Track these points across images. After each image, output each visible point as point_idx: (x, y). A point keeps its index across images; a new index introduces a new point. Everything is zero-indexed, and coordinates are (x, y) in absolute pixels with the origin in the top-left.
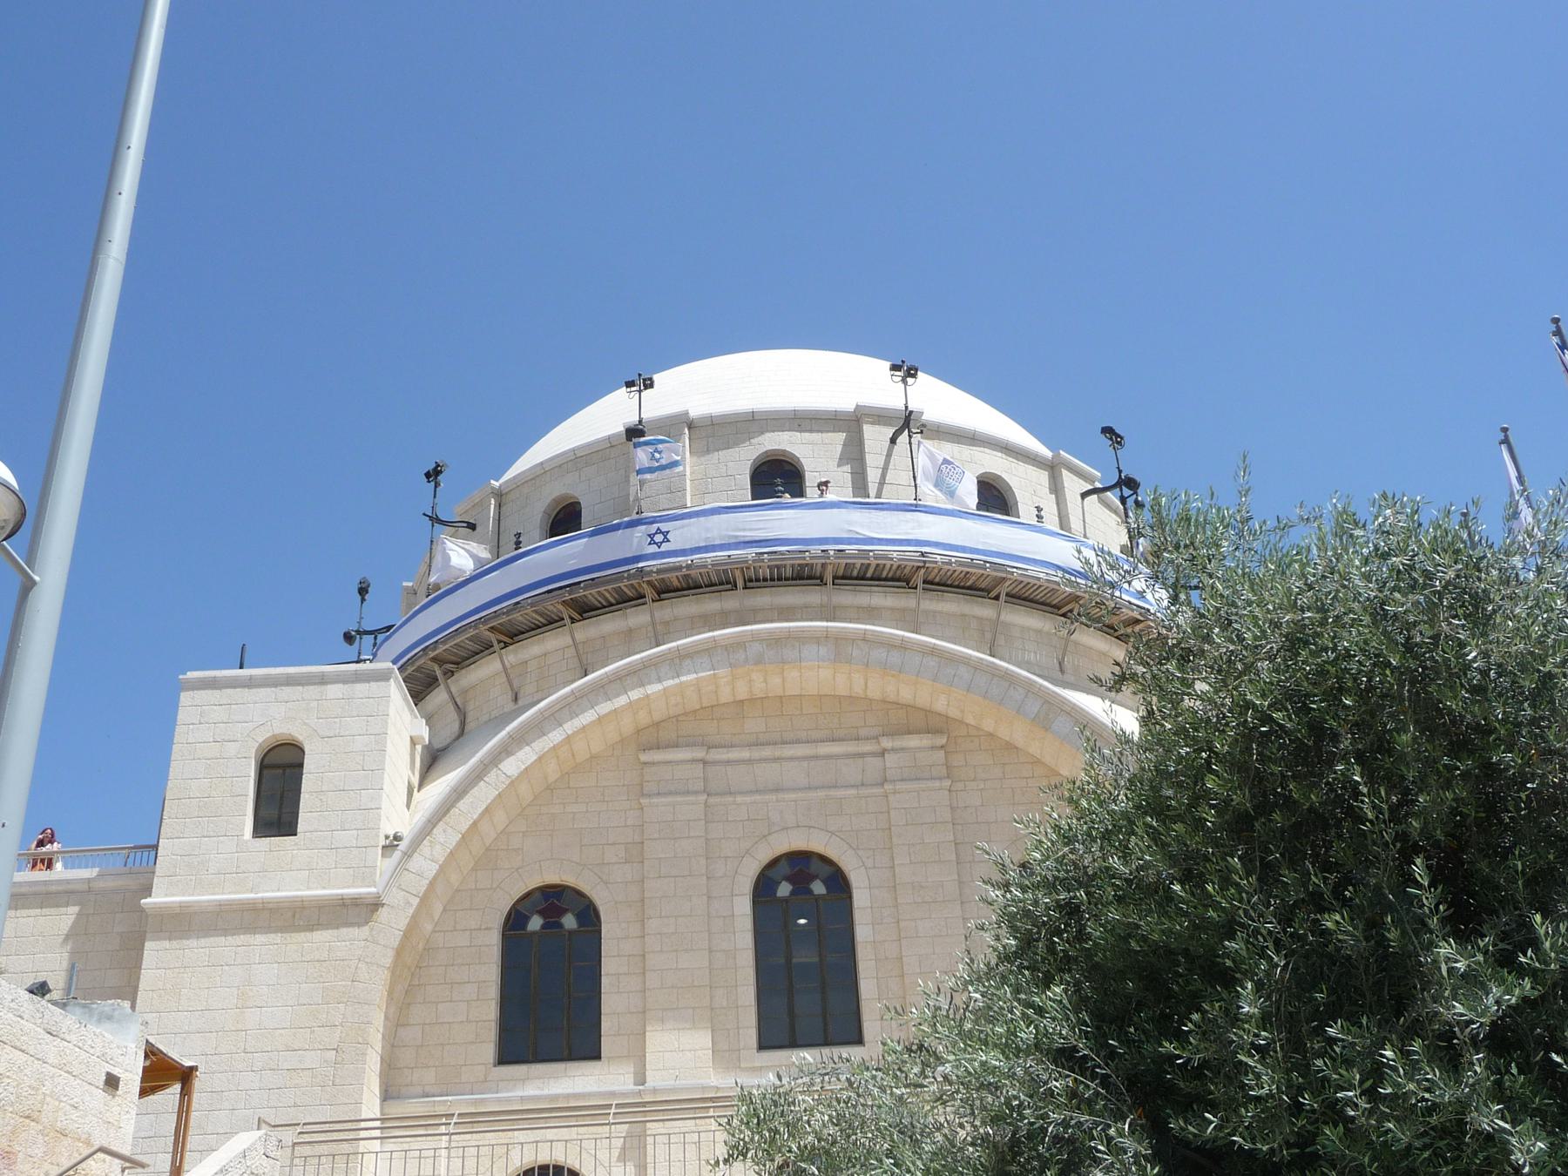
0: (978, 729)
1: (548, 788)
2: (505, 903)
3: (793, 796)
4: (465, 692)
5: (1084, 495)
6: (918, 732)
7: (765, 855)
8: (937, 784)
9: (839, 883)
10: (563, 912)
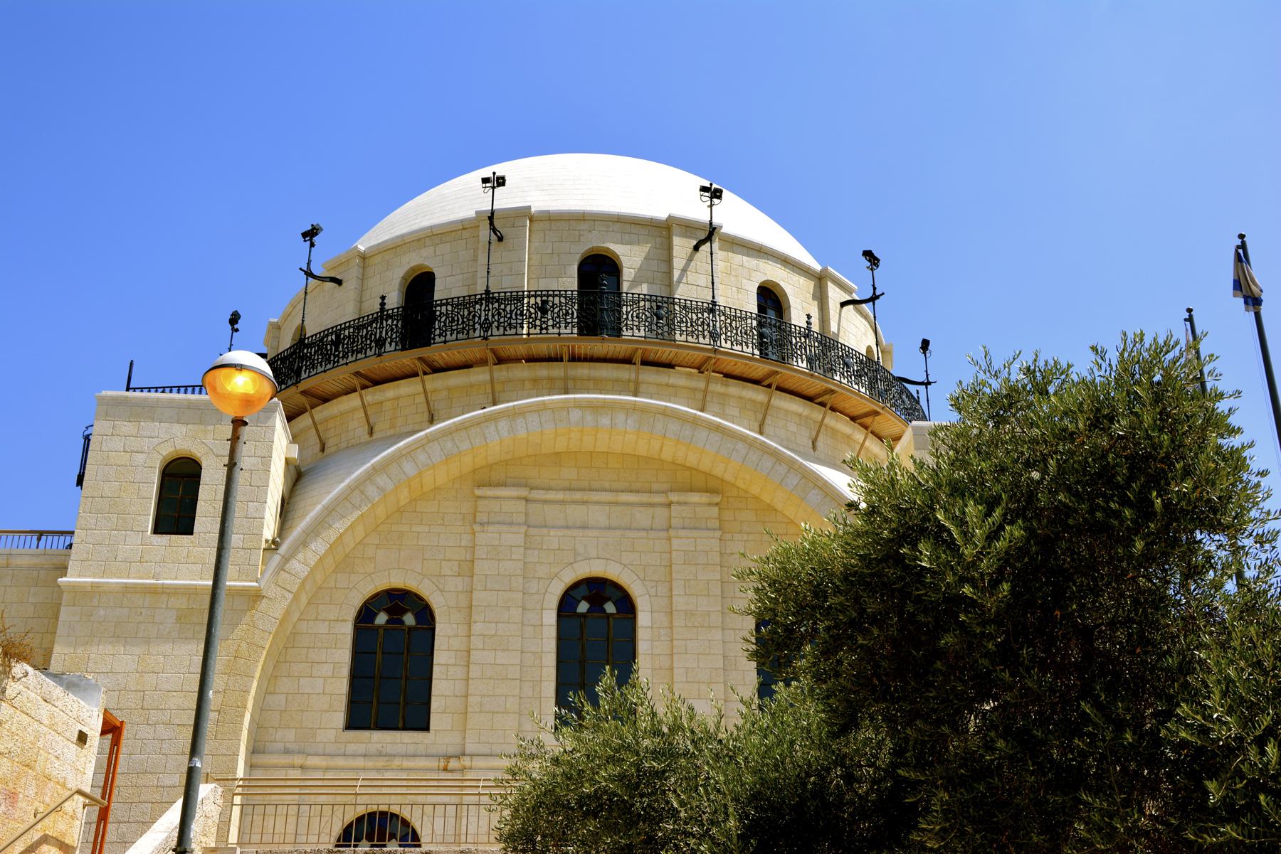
0: (746, 492)
1: (398, 510)
2: (357, 601)
3: (595, 533)
4: (326, 420)
5: (843, 304)
6: (699, 490)
7: (569, 577)
8: (711, 534)
9: (627, 605)
10: (404, 611)
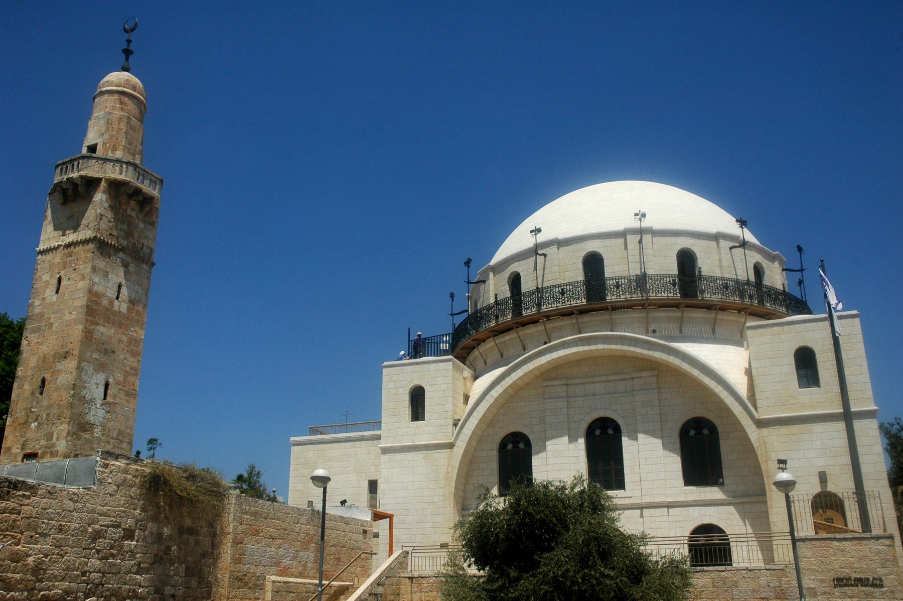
5: (731, 248)
7: (589, 419)
